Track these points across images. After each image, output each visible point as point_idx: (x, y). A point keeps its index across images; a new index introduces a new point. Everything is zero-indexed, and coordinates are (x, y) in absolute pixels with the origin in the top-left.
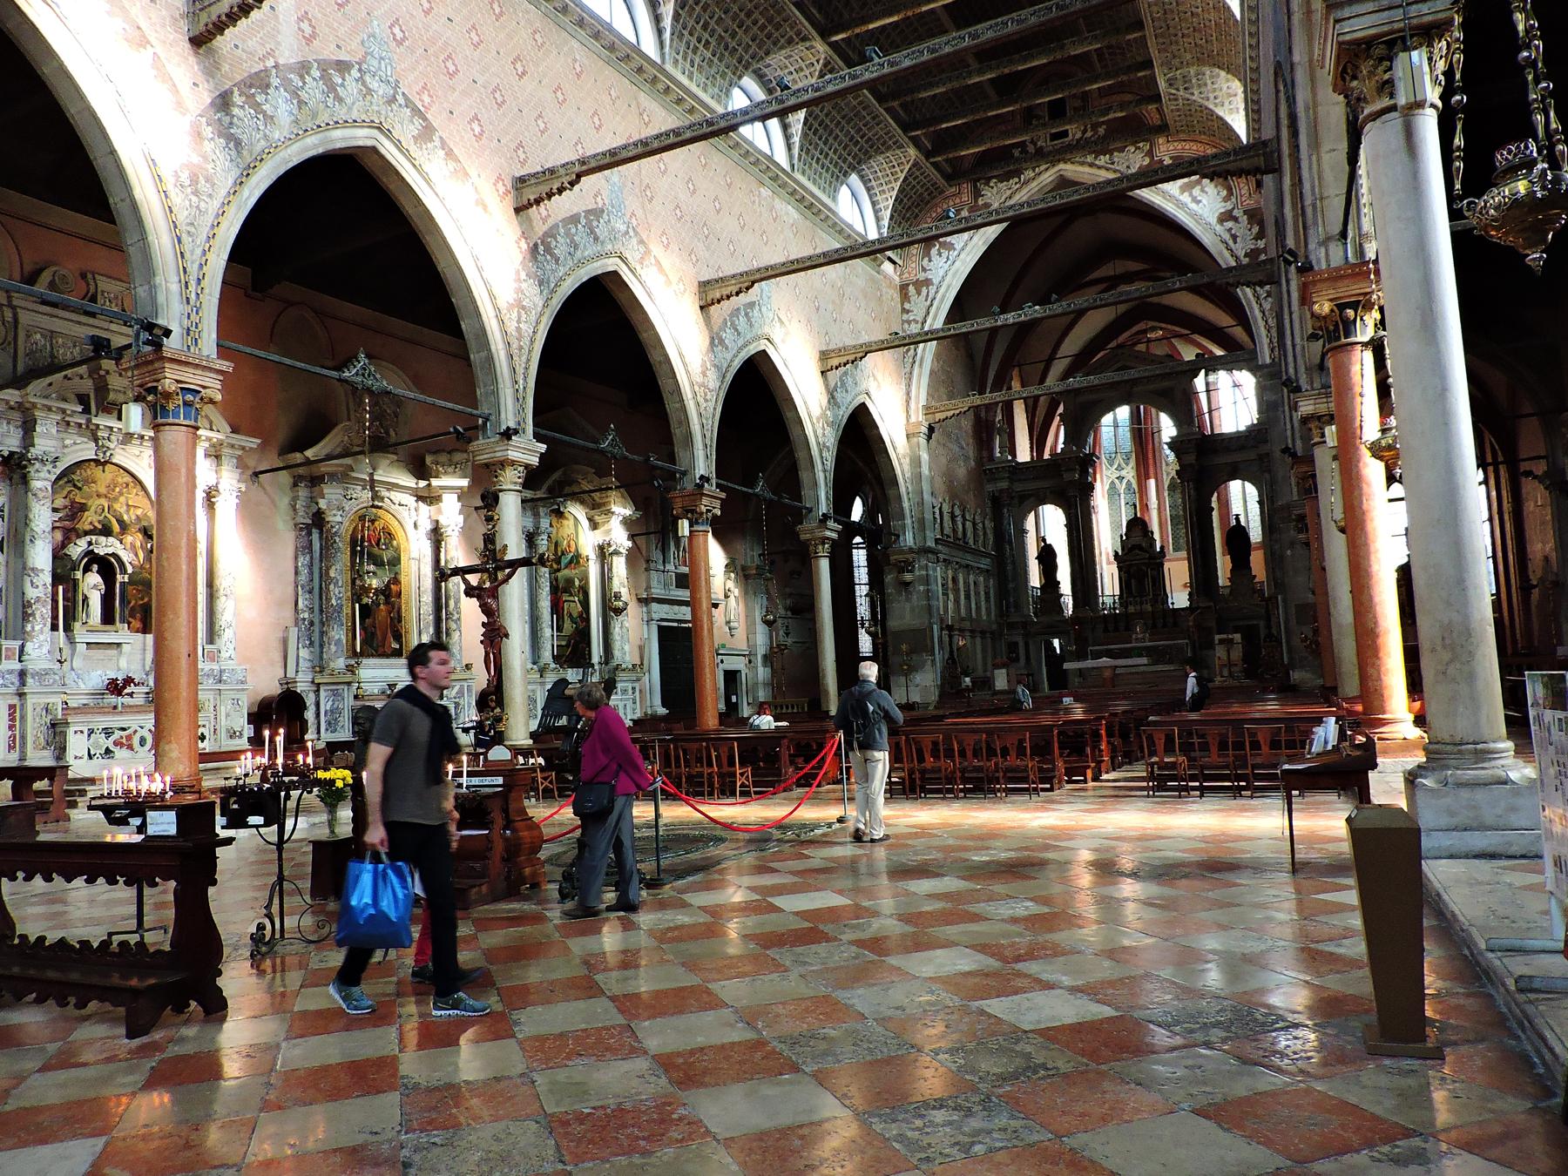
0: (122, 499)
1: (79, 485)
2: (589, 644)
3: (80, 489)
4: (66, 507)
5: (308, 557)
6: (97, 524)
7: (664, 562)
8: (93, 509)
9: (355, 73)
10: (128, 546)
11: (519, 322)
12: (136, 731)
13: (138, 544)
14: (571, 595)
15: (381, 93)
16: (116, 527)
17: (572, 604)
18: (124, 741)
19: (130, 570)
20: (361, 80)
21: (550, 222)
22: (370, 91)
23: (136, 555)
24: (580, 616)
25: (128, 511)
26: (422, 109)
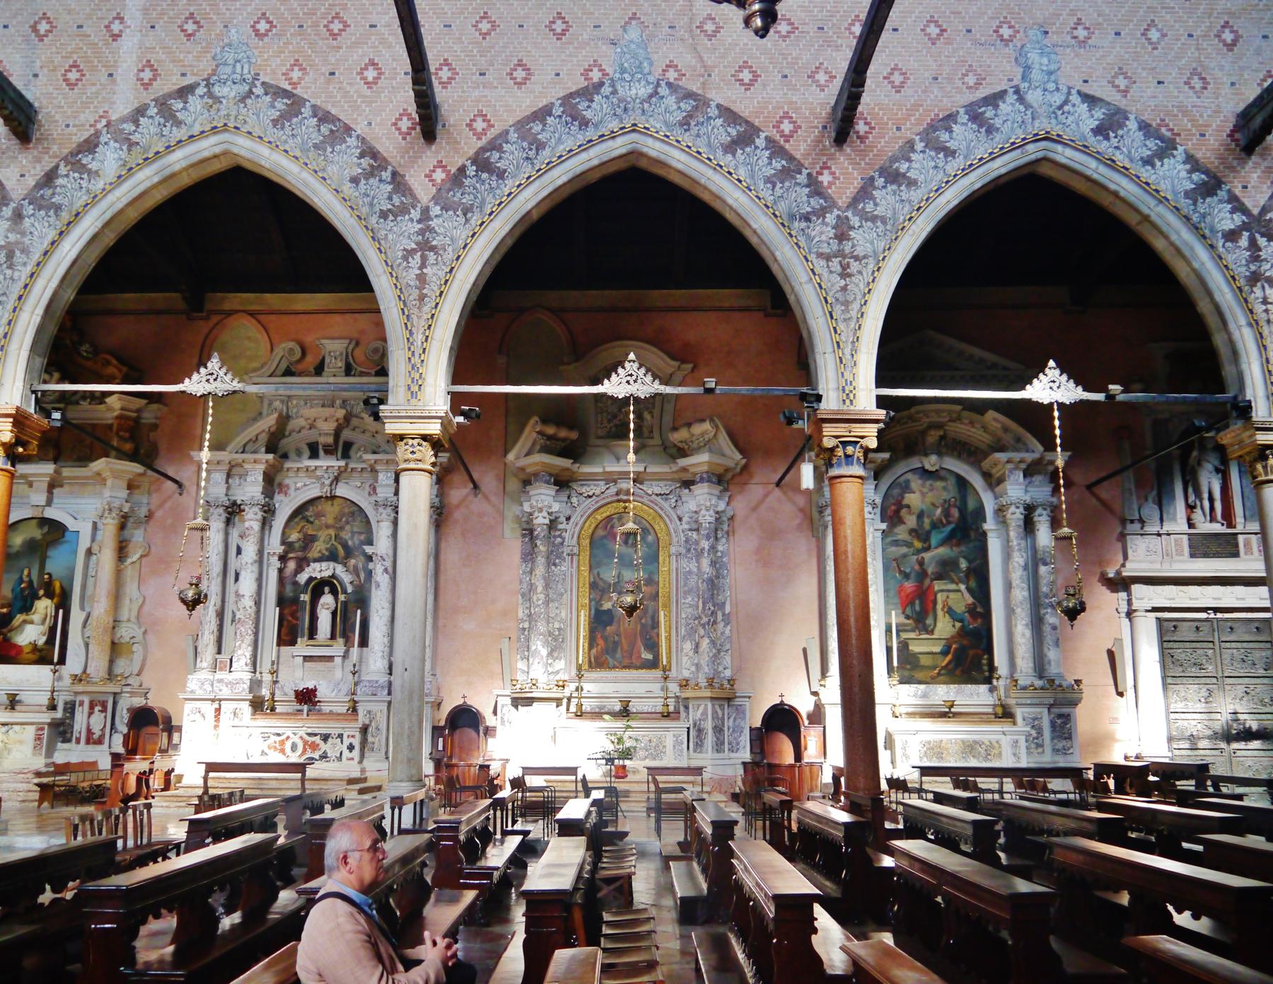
0: (348, 527)
1: (311, 519)
2: (989, 649)
3: (312, 523)
4: (299, 539)
5: (530, 565)
6: (324, 552)
7: (1162, 520)
8: (322, 539)
9: (201, 90)
10: (351, 568)
11: (423, 265)
12: (288, 738)
13: (360, 565)
14: (953, 582)
15: (233, 94)
16: (341, 552)
17: (952, 595)
18: (277, 745)
19: (350, 590)
20: (210, 94)
21: (491, 134)
22: (217, 100)
23: (358, 576)
24: (971, 610)
25: (352, 538)
26: (289, 88)
